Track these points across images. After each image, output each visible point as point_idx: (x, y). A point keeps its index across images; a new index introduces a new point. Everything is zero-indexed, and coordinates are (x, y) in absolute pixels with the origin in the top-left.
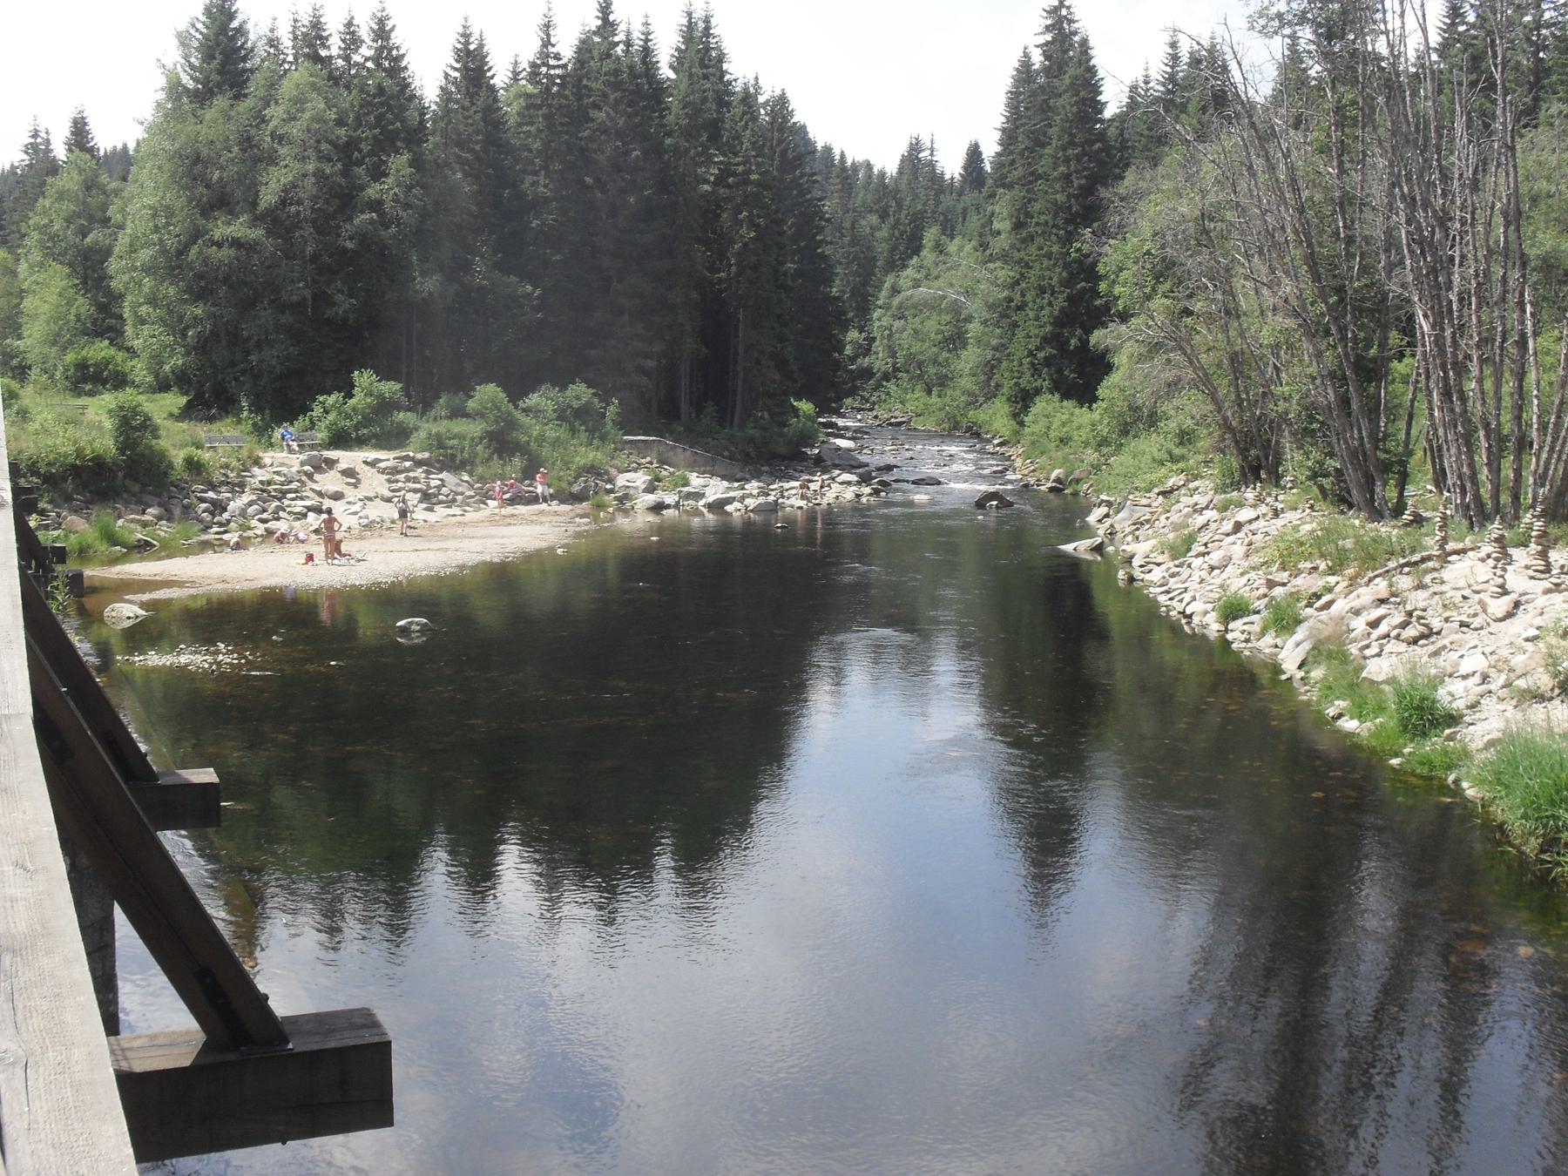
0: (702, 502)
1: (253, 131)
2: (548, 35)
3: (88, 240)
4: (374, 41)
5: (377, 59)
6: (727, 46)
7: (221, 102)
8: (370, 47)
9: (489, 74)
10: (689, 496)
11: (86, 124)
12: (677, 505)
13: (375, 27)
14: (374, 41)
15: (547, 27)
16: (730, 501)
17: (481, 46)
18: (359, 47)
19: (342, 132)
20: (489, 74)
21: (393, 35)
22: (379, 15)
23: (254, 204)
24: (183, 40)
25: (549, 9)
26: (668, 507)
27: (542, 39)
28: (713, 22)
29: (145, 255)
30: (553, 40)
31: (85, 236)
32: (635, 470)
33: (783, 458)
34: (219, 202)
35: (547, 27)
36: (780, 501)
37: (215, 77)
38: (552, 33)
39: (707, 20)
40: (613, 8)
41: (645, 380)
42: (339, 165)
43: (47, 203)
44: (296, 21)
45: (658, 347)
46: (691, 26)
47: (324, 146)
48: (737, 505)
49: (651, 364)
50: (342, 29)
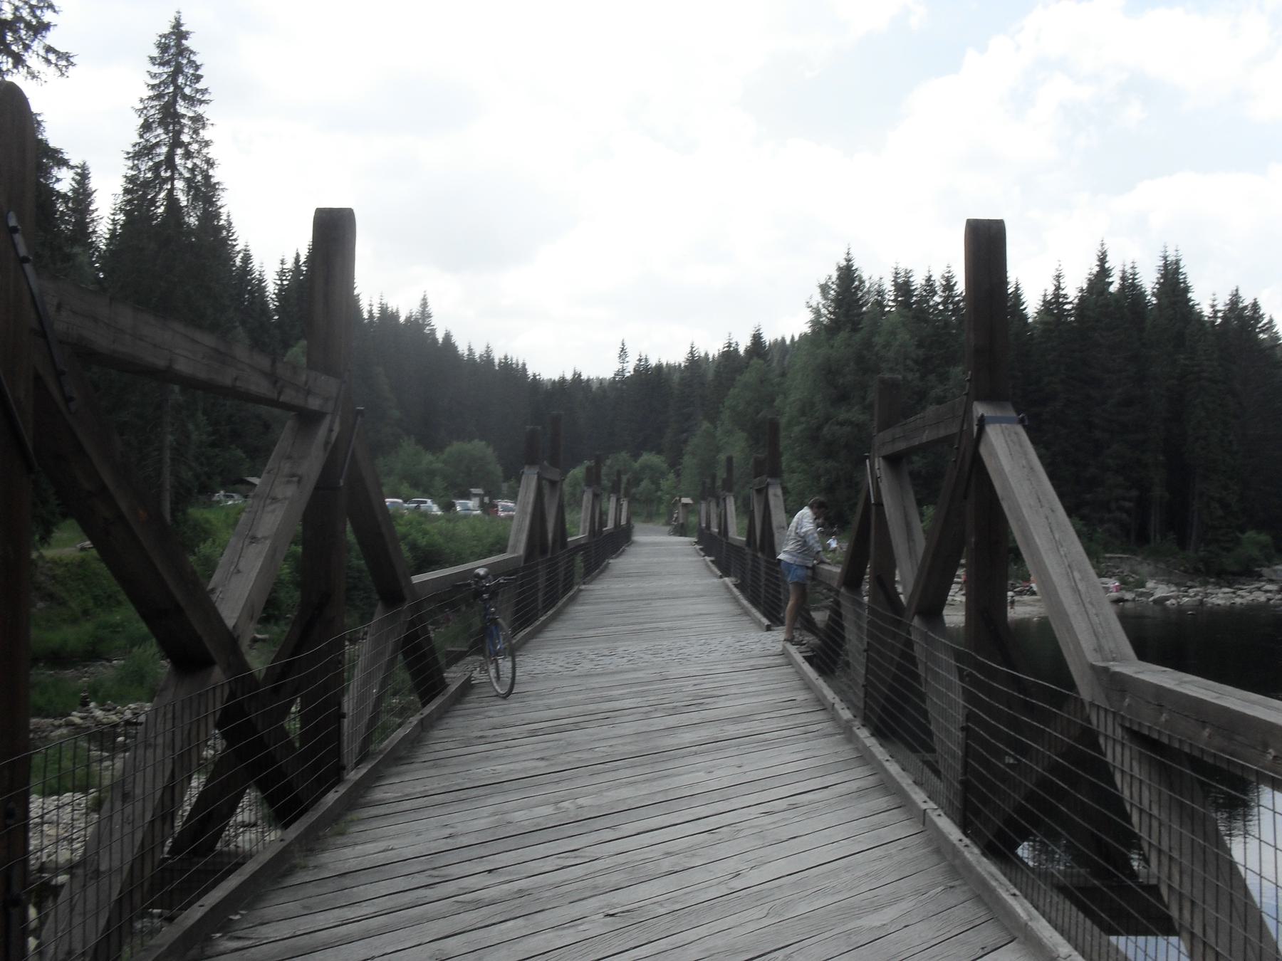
0: (1151, 599)
1: (865, 352)
2: (1059, 283)
3: (760, 416)
4: (943, 292)
5: (944, 303)
6: (1191, 281)
7: (843, 335)
8: (941, 296)
9: (1022, 308)
10: (1142, 594)
11: (761, 338)
12: (1134, 600)
13: (944, 283)
14: (943, 292)
15: (1058, 277)
16: (1167, 598)
17: (1017, 289)
18: (933, 296)
19: (921, 352)
20: (1022, 308)
21: (956, 288)
22: (946, 275)
23: (864, 398)
24: (824, 289)
25: (1060, 265)
26: (1127, 600)
27: (1055, 285)
28: (1182, 264)
29: (797, 429)
30: (1062, 286)
31: (758, 413)
32: (1110, 577)
33: (1234, 574)
34: (842, 398)
35: (1058, 277)
36: (1205, 599)
37: (842, 319)
38: (1061, 281)
39: (1177, 262)
40: (1108, 259)
41: (1124, 516)
42: (918, 375)
43: (737, 390)
44: (897, 273)
45: (1134, 493)
46: (1166, 266)
47: (909, 362)
48: (1173, 601)
49: (1127, 504)
50: (924, 282)
